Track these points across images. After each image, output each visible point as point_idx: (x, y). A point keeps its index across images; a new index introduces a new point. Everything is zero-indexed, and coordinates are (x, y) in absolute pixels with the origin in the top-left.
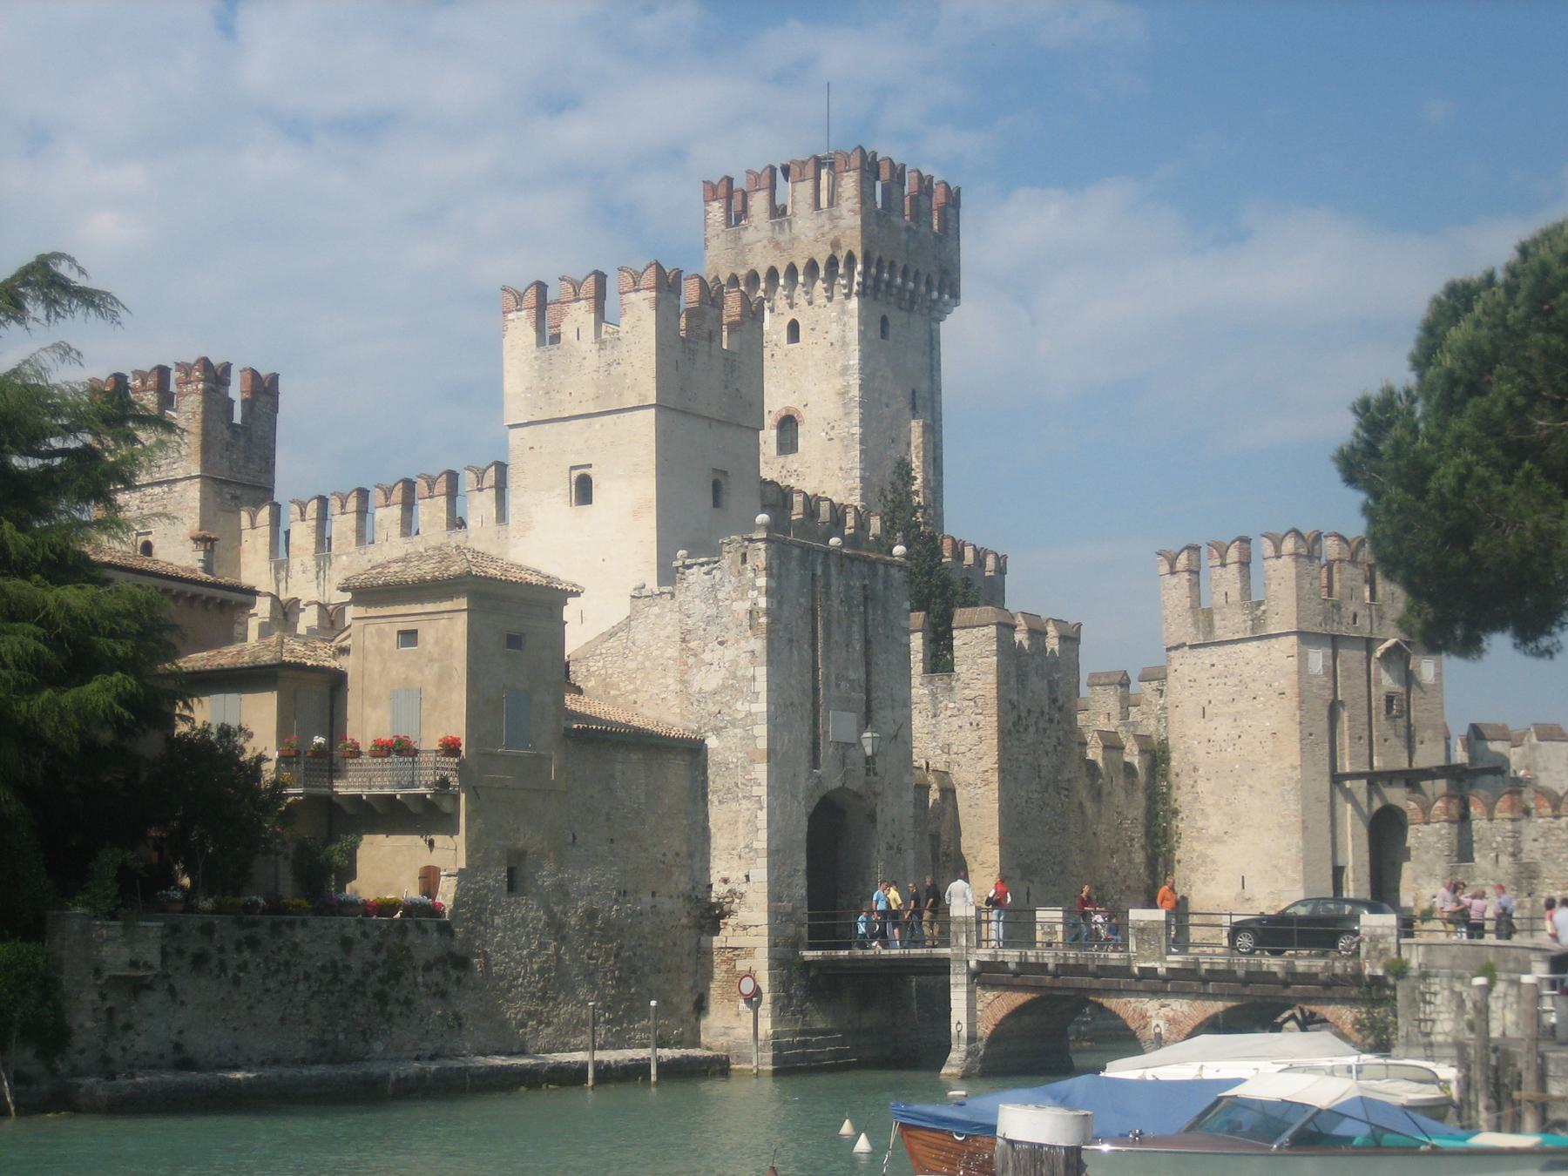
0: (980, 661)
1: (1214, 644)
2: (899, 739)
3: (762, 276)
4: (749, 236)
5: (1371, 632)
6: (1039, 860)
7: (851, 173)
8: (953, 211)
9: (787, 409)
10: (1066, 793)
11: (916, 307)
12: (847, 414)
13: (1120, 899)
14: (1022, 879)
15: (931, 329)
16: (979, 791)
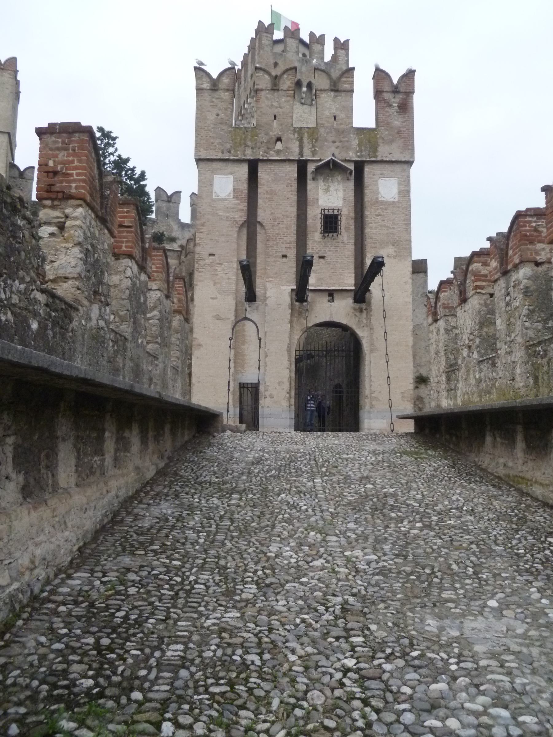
5: (301, 154)
8: (343, 52)
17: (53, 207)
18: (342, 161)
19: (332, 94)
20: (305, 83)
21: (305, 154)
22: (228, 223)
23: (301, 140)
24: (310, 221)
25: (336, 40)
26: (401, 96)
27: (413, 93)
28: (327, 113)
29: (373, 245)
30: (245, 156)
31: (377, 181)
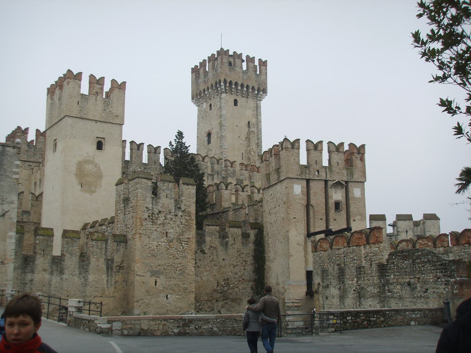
0: (134, 192)
1: (271, 186)
2: (6, 217)
3: (202, 92)
4: (200, 81)
6: (164, 269)
7: (220, 56)
8: (264, 67)
9: (209, 130)
10: (186, 243)
11: (249, 96)
12: (221, 129)
13: (238, 284)
14: (151, 276)
15: (257, 104)
16: (132, 242)
17: (377, 244)
18: (342, 181)
19: (337, 153)
20: (245, 86)
21: (327, 177)
22: (300, 205)
23: (326, 172)
24: (330, 205)
25: (260, 60)
26: (361, 155)
27: (365, 153)
28: (335, 161)
29: (353, 215)
30: (306, 177)
31: (353, 189)
